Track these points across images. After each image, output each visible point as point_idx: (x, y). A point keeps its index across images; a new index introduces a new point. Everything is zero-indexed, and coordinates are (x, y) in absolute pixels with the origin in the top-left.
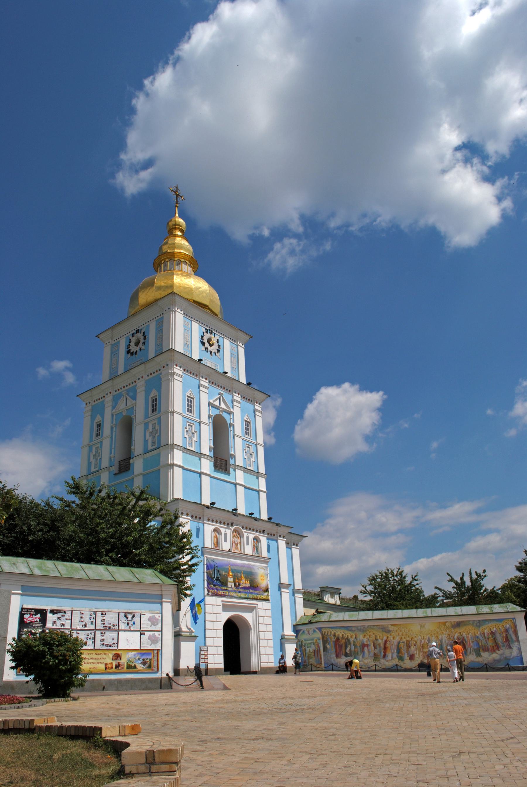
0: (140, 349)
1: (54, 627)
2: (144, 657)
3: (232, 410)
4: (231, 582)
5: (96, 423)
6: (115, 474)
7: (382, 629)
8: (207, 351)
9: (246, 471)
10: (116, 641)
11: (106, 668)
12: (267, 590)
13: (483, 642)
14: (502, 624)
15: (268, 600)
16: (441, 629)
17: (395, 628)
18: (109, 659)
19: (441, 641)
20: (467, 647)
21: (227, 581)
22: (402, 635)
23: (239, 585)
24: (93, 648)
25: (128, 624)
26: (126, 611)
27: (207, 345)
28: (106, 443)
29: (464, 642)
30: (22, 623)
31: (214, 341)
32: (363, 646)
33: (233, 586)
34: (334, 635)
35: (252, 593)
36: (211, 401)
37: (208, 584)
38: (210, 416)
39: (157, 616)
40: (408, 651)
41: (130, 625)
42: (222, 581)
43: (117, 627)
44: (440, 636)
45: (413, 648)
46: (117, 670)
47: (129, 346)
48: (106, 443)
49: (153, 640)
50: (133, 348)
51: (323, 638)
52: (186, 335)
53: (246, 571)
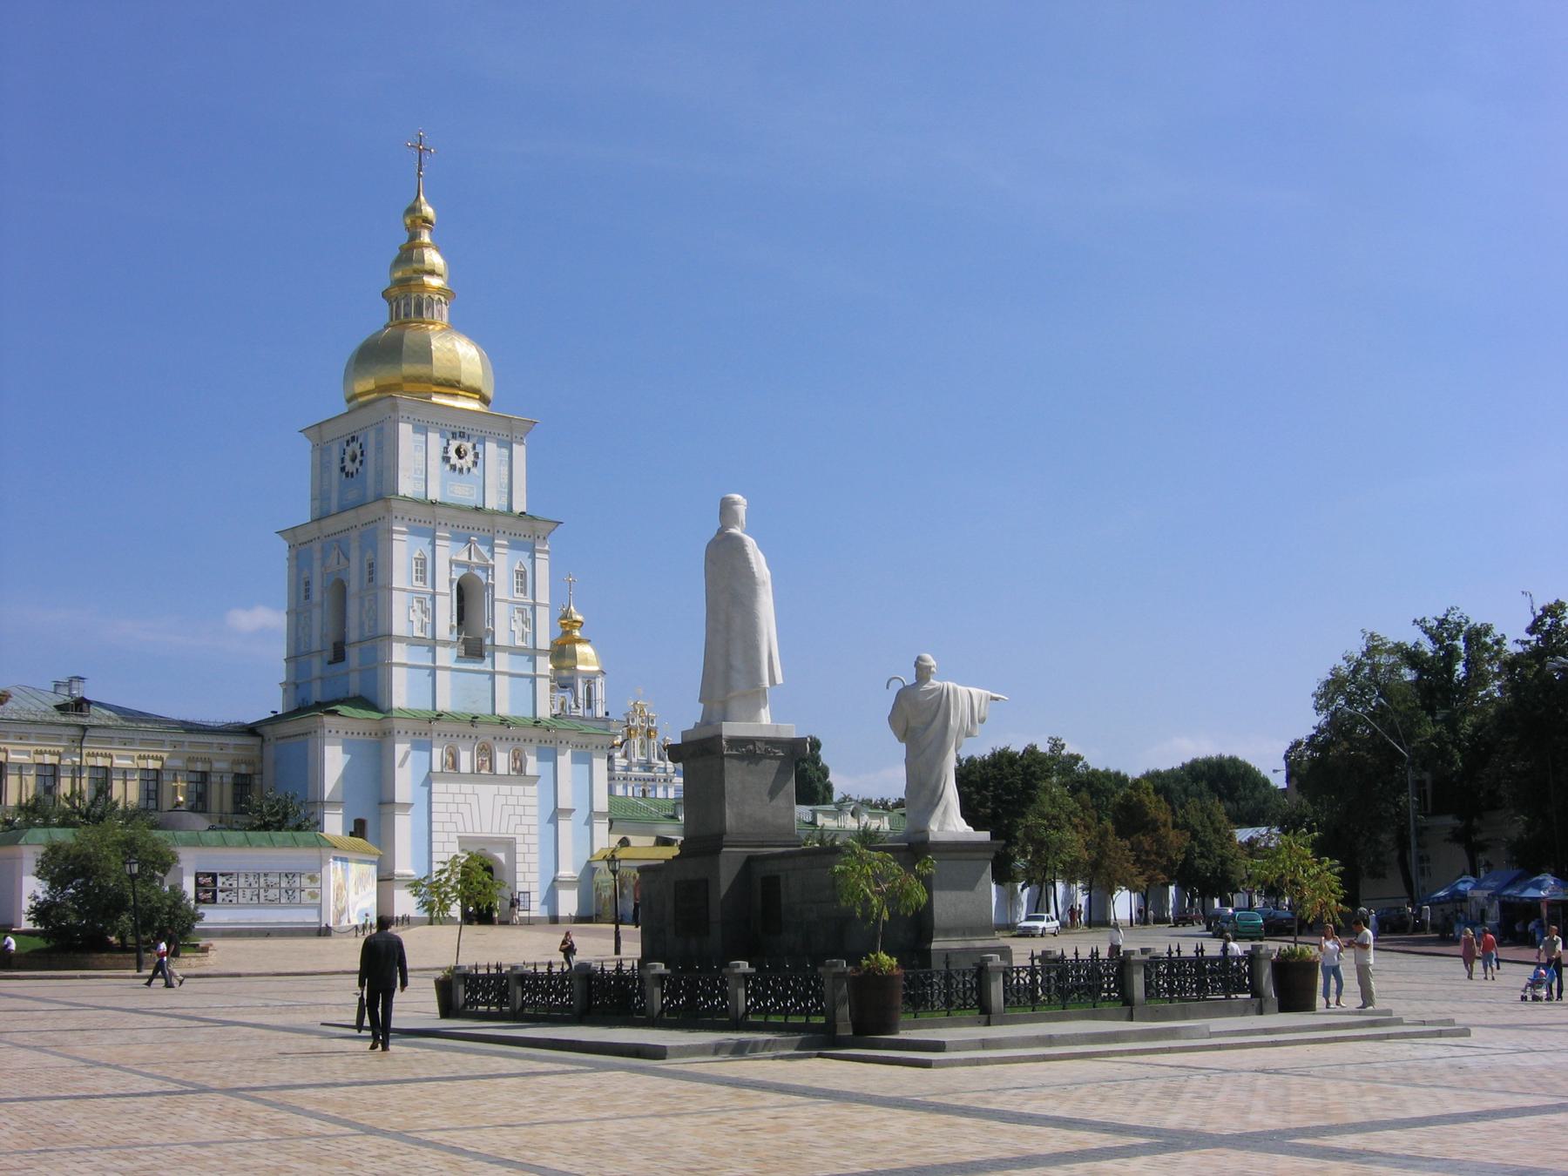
0: (357, 470)
3: (491, 562)
5: (305, 578)
6: (330, 663)
8: (455, 470)
9: (513, 651)
10: (278, 897)
28: (317, 614)
30: (198, 884)
36: (454, 557)
38: (451, 582)
41: (291, 882)
47: (343, 460)
48: (317, 614)
49: (313, 895)
50: (350, 467)
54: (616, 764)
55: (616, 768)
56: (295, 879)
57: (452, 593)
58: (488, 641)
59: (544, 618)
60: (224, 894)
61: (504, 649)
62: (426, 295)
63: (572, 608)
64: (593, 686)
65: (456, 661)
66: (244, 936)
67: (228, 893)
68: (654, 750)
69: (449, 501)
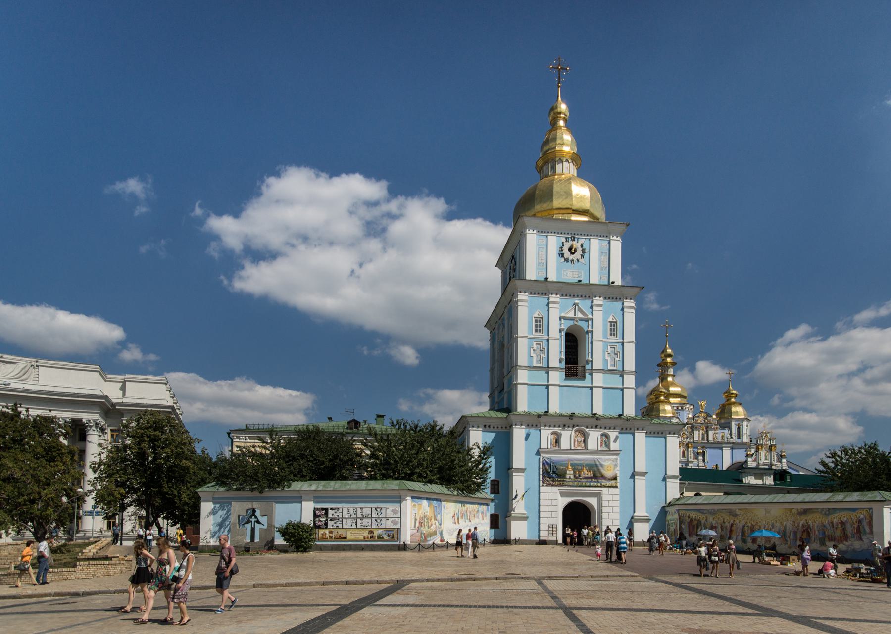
1: (333, 517)
2: (389, 533)
4: (570, 474)
7: (730, 512)
10: (370, 523)
11: (364, 538)
12: (615, 478)
14: (854, 514)
15: (617, 487)
16: (786, 516)
17: (742, 513)
18: (366, 533)
19: (785, 527)
20: (811, 535)
21: (566, 473)
22: (748, 519)
23: (580, 476)
24: (355, 527)
25: (377, 514)
26: (376, 506)
29: (809, 530)
33: (572, 477)
35: (595, 482)
37: (543, 477)
39: (397, 509)
41: (379, 514)
42: (559, 474)
43: (370, 516)
44: (785, 523)
46: (371, 540)
49: (395, 523)
53: (589, 464)
56: (382, 511)
60: (333, 522)
66: (340, 550)
67: (335, 521)
68: (774, 457)
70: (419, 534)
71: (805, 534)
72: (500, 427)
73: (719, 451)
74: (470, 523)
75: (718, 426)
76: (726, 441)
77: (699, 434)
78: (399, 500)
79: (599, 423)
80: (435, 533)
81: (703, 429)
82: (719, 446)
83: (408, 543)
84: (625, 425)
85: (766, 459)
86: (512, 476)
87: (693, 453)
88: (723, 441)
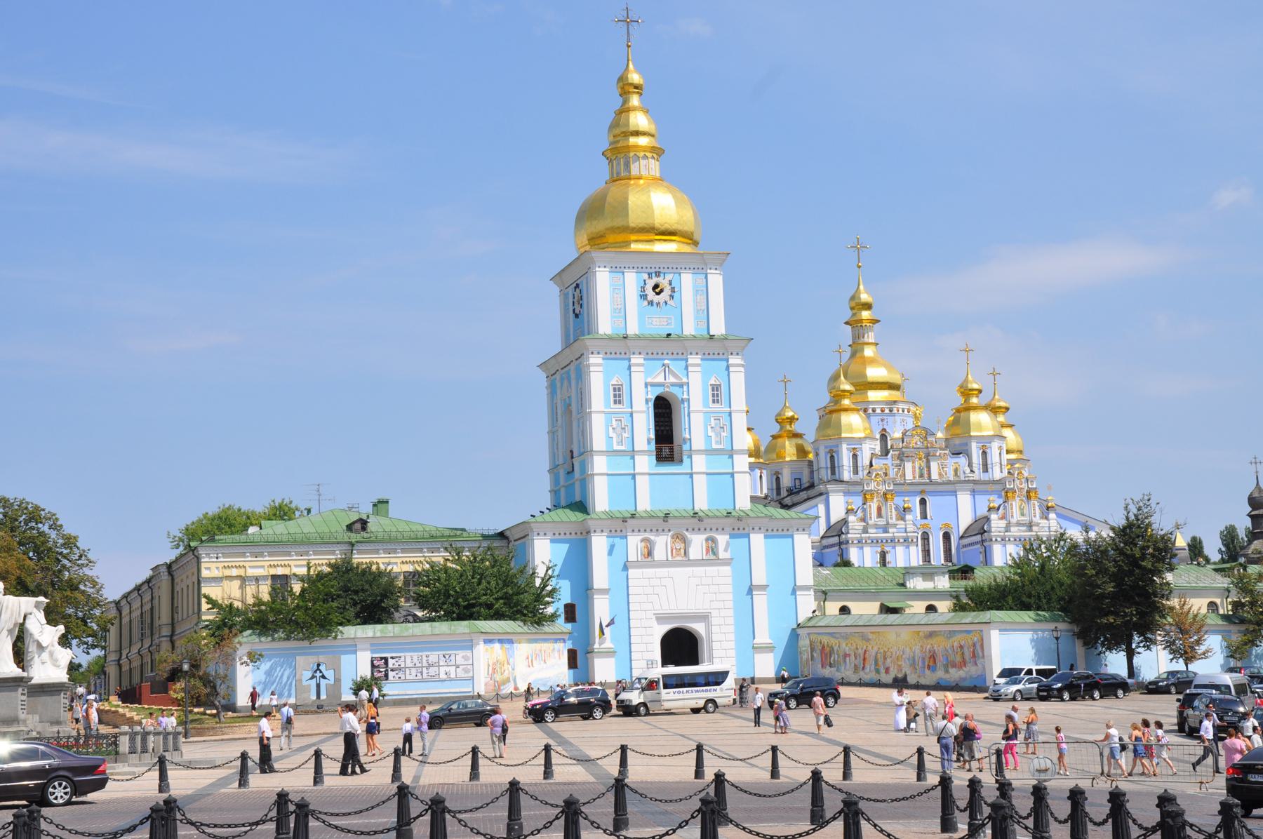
3: (685, 380)
6: (568, 473)
8: (652, 305)
9: (709, 452)
13: (952, 658)
17: (874, 636)
19: (914, 653)
26: (444, 652)
27: (651, 294)
30: (373, 666)
31: (664, 282)
32: (846, 655)
34: (821, 643)
36: (649, 380)
38: (647, 401)
40: (884, 663)
45: (889, 660)
47: (573, 303)
49: (466, 671)
51: (811, 645)
52: (616, 296)
54: (992, 525)
55: (993, 530)
57: (648, 408)
58: (686, 447)
59: (740, 421)
60: (394, 673)
61: (699, 452)
62: (632, 154)
63: (969, 376)
64: (988, 451)
65: (656, 466)
69: (647, 332)
70: (492, 682)
71: (932, 659)
72: (573, 533)
73: (951, 498)
74: (545, 665)
75: (947, 452)
76: (962, 478)
77: (914, 468)
78: (470, 647)
79: (702, 525)
80: (508, 680)
81: (920, 459)
82: (950, 488)
83: (482, 693)
84: (737, 524)
85: (1023, 515)
86: (593, 599)
87: (897, 509)
88: (957, 479)
